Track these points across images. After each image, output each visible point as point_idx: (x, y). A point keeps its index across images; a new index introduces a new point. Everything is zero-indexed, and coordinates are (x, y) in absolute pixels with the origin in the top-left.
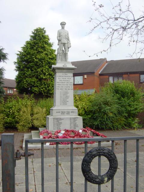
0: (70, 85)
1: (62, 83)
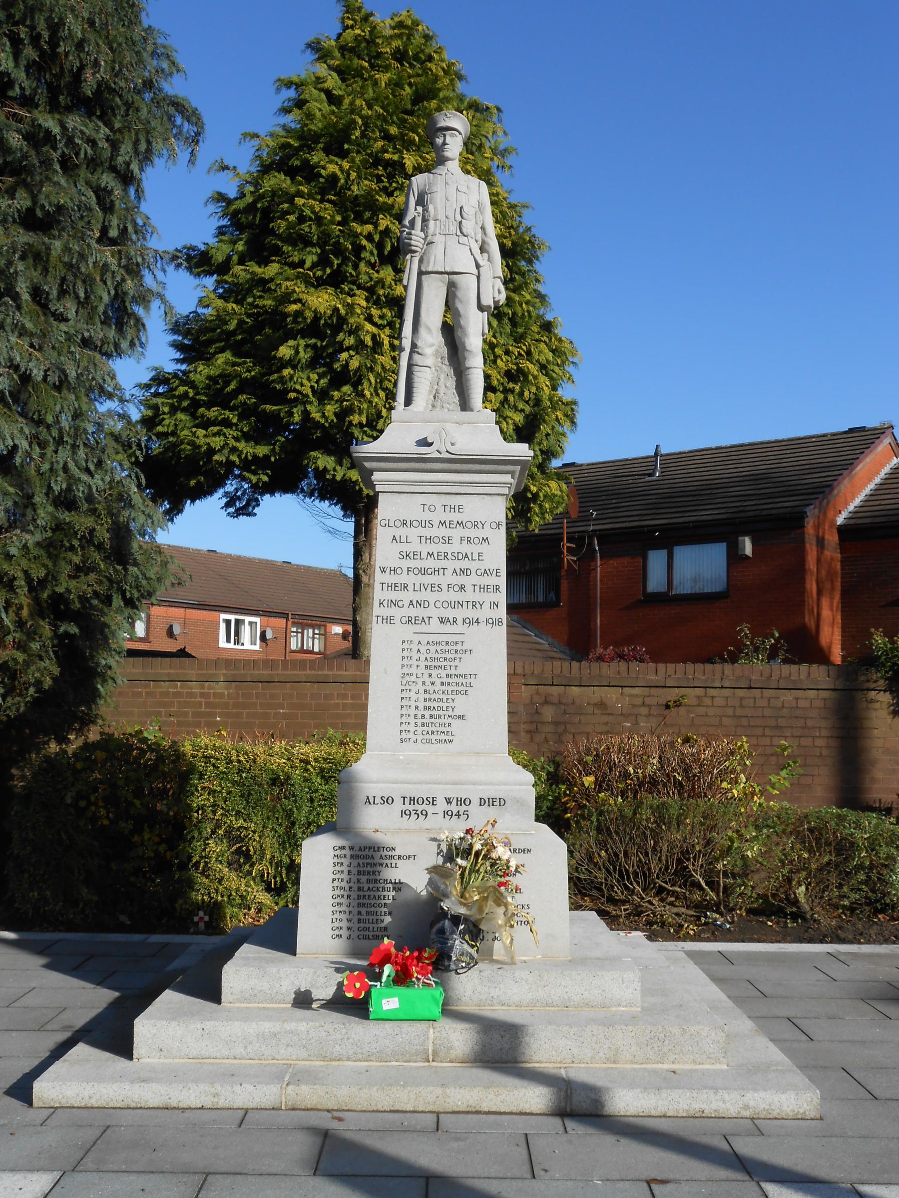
0: (484, 588)
1: (423, 572)
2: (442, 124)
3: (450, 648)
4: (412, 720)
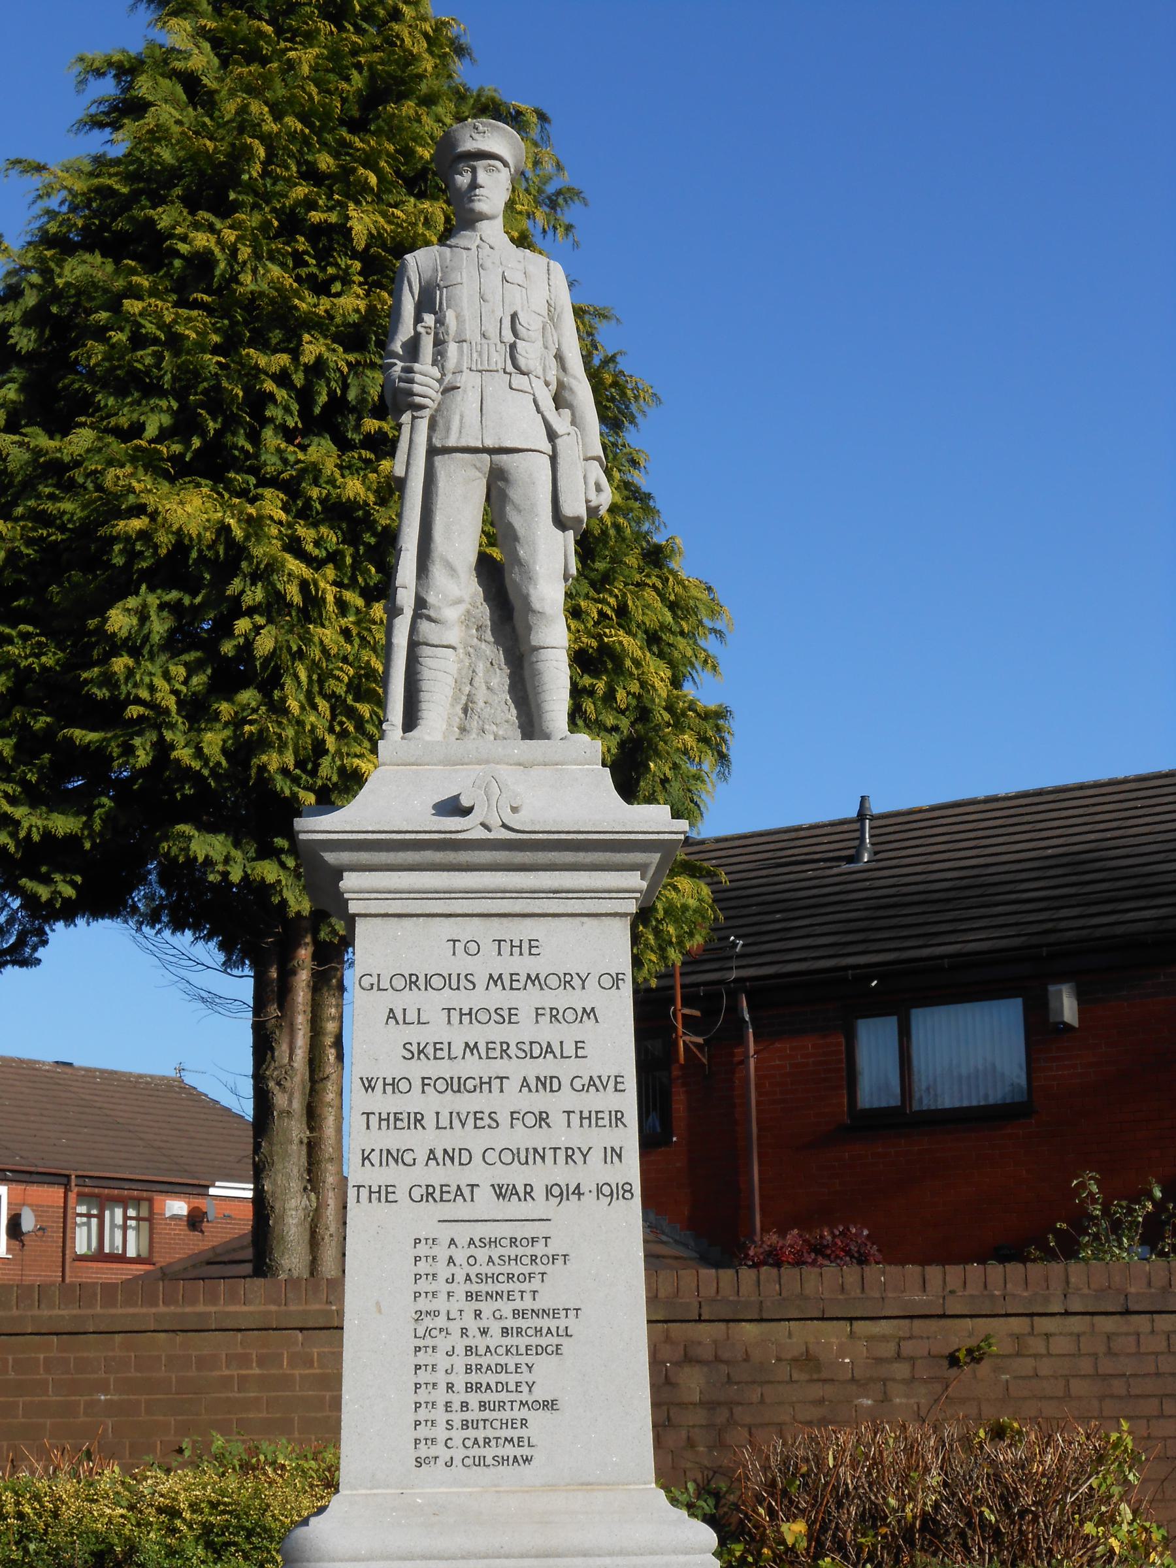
0: (590, 1119)
1: (457, 1086)
2: (468, 145)
3: (520, 1251)
4: (440, 1416)
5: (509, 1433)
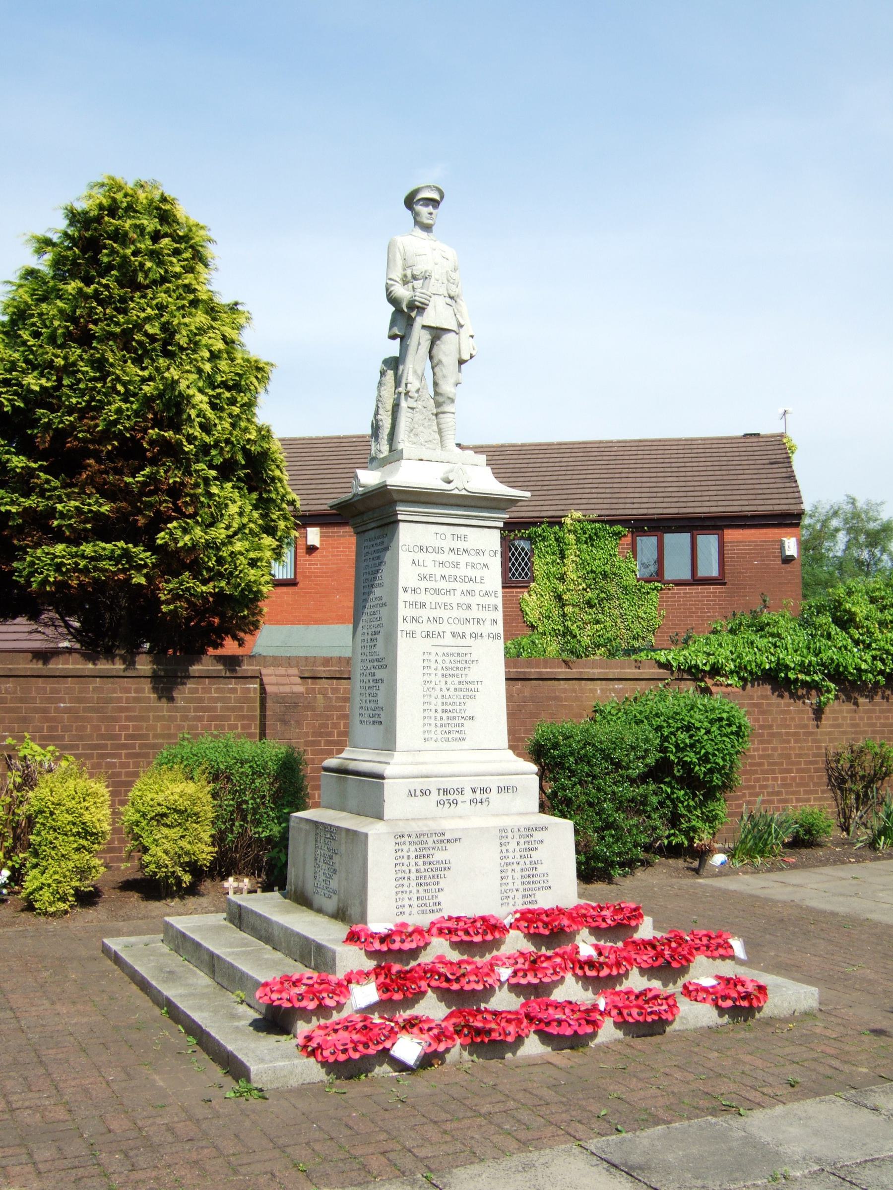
0: (486, 607)
1: (437, 592)
4: (433, 722)
5: (457, 729)
